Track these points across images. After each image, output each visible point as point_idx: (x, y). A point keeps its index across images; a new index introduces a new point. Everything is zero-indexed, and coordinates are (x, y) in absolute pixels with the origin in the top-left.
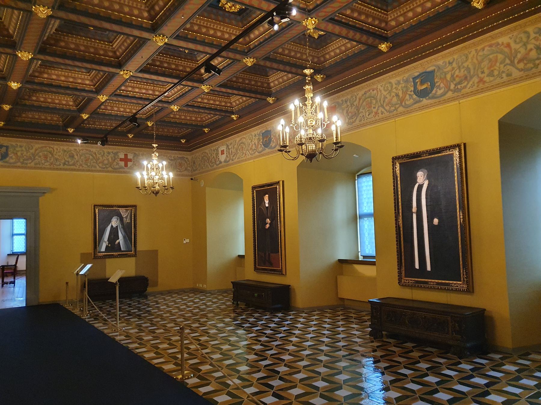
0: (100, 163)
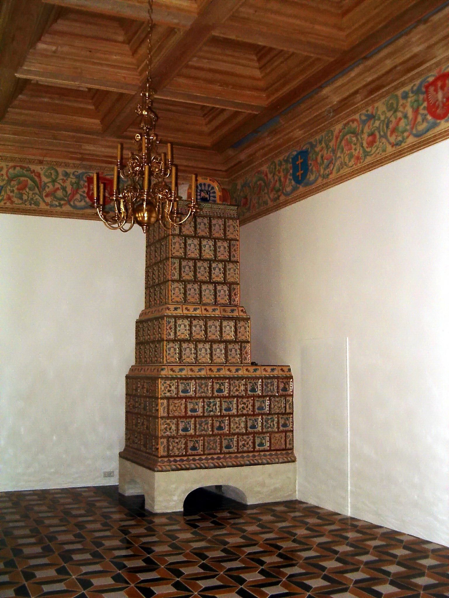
0: (47, 196)
